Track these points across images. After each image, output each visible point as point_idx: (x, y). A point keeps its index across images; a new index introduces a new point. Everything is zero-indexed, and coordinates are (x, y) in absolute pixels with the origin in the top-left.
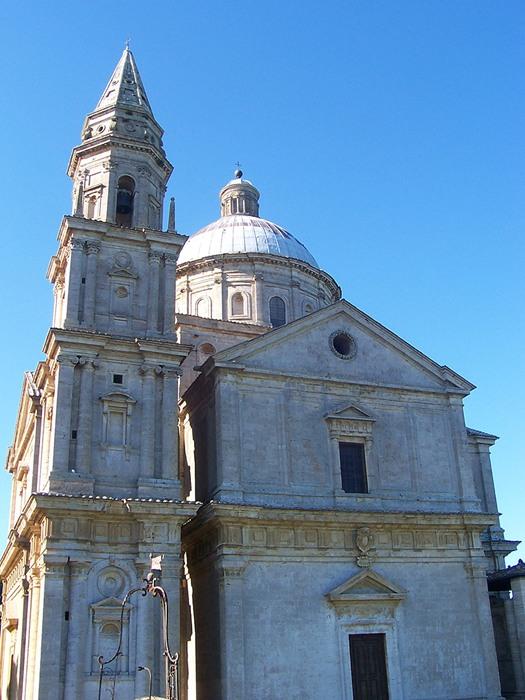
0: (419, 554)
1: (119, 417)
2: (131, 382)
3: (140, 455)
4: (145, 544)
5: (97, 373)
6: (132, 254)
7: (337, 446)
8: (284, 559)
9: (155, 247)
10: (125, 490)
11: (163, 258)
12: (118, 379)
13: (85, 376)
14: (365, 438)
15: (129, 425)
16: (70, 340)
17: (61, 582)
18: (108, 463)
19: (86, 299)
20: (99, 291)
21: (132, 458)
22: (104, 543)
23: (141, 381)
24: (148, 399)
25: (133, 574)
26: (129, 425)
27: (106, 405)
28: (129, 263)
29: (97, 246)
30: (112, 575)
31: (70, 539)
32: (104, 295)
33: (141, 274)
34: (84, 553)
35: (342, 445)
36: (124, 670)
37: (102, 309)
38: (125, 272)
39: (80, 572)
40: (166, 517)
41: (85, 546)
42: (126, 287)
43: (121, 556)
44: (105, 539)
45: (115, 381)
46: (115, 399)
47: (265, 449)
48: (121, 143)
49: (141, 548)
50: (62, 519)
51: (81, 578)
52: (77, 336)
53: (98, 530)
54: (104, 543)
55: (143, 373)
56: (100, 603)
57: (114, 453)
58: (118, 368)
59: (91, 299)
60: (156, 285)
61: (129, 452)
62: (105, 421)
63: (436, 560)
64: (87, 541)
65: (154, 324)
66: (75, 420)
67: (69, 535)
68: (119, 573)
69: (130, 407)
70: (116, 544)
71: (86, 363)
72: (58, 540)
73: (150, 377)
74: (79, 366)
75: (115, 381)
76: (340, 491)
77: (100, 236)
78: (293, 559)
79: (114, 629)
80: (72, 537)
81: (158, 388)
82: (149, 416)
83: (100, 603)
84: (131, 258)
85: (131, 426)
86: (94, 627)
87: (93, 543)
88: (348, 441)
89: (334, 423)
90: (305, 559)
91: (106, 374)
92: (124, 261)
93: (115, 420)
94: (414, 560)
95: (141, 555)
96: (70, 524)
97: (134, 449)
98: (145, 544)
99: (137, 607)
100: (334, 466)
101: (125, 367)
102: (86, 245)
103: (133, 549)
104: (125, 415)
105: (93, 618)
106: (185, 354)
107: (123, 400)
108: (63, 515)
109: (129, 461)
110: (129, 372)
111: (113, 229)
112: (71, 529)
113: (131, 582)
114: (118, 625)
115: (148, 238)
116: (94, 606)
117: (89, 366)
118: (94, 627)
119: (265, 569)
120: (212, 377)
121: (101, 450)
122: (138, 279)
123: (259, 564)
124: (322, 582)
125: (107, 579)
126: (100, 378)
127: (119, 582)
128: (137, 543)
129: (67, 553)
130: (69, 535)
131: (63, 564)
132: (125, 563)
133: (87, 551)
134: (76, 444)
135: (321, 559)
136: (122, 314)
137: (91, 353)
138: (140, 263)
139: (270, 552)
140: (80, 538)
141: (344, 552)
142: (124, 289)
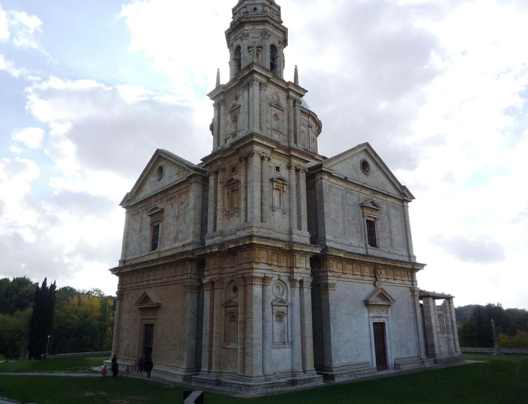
4: (296, 268)
6: (280, 95)
8: (349, 280)
9: (291, 94)
10: (285, 235)
11: (295, 101)
17: (261, 289)
23: (288, 172)
24: (294, 183)
25: (288, 285)
30: (279, 285)
36: (286, 341)
41: (271, 268)
42: (278, 115)
43: (283, 274)
48: (272, 22)
55: (289, 167)
65: (292, 139)
67: (264, 261)
70: (280, 267)
73: (293, 171)
78: (352, 280)
82: (294, 192)
84: (279, 97)
90: (356, 281)
92: (275, 98)
94: (392, 284)
95: (295, 274)
97: (287, 212)
98: (296, 268)
99: (292, 304)
103: (288, 270)
109: (284, 218)
114: (282, 314)
115: (290, 87)
116: (274, 303)
119: (341, 284)
122: (282, 110)
123: (340, 282)
124: (364, 295)
127: (281, 288)
128: (293, 267)
129: (263, 271)
133: (271, 270)
135: (362, 281)
138: (283, 102)
139: (344, 276)
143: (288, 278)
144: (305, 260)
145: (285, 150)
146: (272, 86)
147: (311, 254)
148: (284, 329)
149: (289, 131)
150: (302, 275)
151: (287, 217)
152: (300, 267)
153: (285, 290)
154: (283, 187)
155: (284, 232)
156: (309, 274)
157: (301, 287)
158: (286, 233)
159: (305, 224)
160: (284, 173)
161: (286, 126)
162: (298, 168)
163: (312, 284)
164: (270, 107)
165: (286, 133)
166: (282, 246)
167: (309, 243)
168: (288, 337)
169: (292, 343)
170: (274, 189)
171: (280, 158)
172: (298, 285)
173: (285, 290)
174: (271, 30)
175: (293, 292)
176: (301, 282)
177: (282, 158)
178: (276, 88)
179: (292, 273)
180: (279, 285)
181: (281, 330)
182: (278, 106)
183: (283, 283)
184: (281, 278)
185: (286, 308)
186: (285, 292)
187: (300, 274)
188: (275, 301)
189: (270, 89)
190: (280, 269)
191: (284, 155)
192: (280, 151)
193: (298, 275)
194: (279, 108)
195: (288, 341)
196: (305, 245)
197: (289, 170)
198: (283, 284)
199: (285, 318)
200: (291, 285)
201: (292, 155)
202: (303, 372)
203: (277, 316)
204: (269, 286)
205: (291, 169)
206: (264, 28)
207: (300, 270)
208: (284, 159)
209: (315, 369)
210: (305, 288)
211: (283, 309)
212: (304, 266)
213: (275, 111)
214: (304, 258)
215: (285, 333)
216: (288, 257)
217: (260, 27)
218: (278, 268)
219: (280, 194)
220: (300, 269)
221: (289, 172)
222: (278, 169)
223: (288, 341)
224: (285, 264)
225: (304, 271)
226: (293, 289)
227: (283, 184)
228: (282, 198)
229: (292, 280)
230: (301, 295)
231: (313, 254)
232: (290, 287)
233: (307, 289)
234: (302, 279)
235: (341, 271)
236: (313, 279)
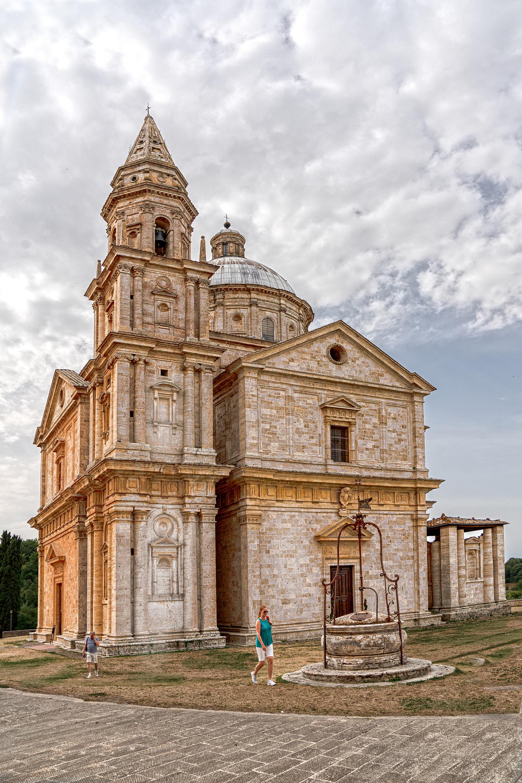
0: (381, 508)
1: (166, 403)
2: (174, 377)
3: (183, 431)
4: (190, 497)
5: (148, 368)
6: (171, 279)
7: (329, 429)
12: (164, 373)
13: (138, 370)
14: (349, 422)
15: (174, 408)
16: (126, 342)
18: (159, 436)
19: (136, 312)
20: (145, 306)
21: (177, 432)
22: (158, 496)
23: (182, 375)
25: (180, 520)
26: (174, 408)
27: (156, 392)
28: (169, 285)
29: (143, 271)
30: (165, 520)
31: (134, 494)
32: (150, 309)
33: (180, 294)
34: (145, 504)
35: (333, 428)
37: (149, 319)
38: (166, 292)
39: (142, 518)
40: (206, 477)
42: (168, 304)
44: (159, 493)
45: (162, 375)
46: (162, 388)
47: (276, 428)
49: (187, 500)
50: (127, 478)
51: (143, 524)
52: (132, 339)
53: (154, 486)
54: (158, 496)
55: (184, 369)
56: (157, 542)
57: (163, 431)
58: (163, 364)
59: (140, 312)
60: (192, 301)
61: (175, 428)
62: (155, 404)
63: (392, 512)
64: (147, 494)
66: (133, 403)
68: (168, 519)
69: (175, 394)
70: (167, 497)
71: (140, 360)
72: (124, 494)
74: (133, 363)
75: (162, 375)
76: (330, 462)
77: (144, 263)
79: (165, 561)
80: (136, 492)
81: (196, 381)
82: (191, 401)
83: (157, 542)
85: (176, 408)
86: (152, 560)
87: (151, 496)
88: (337, 424)
89: (328, 411)
91: (154, 369)
93: (164, 404)
96: (133, 481)
98: (190, 497)
99: (184, 545)
100: (326, 441)
101: (170, 364)
102: (132, 270)
103: (180, 501)
104: (170, 400)
105: (152, 552)
106: (218, 356)
107: (169, 389)
108: (127, 475)
109: (175, 434)
110: (174, 368)
111: (155, 258)
112: (134, 485)
113: (178, 526)
116: (154, 544)
117: (141, 362)
118: (152, 560)
120: (236, 376)
121: (156, 426)
125: (160, 524)
126: (150, 372)
127: (170, 526)
128: (185, 496)
130: (133, 490)
131: (127, 512)
132: (174, 511)
134: (134, 421)
136: (166, 324)
137: (143, 353)
140: (142, 492)
141: (331, 506)
142: (165, 305)
143: (179, 512)
144: (205, 485)
145: (172, 347)
146: (157, 270)
147: (215, 477)
148: (173, 577)
149: (187, 321)
150: (200, 506)
151: (179, 433)
152: (195, 496)
153: (175, 526)
154: (172, 395)
155: (171, 452)
156: (213, 504)
157: (199, 523)
158: (175, 452)
159: (208, 439)
160: (174, 377)
161: (182, 316)
162: (198, 367)
163: (218, 518)
164: (153, 297)
165: (182, 325)
166: (160, 470)
167: (215, 464)
168: (178, 587)
169: (183, 595)
170: (155, 399)
171: (169, 358)
172: (192, 519)
173: (175, 526)
174: (157, 200)
175: (185, 529)
176: (199, 515)
177: (172, 359)
178: (163, 271)
179: (184, 504)
180: (165, 520)
181: (168, 578)
182: (166, 292)
183: (171, 519)
184: (168, 512)
185: (175, 550)
186: (175, 530)
187: (196, 505)
188: (155, 540)
189: (153, 274)
190: (165, 500)
191: (174, 353)
192: (165, 350)
193: (192, 506)
194: (168, 295)
195: (178, 593)
196: (208, 466)
197: (185, 372)
198: (172, 520)
199: (174, 562)
200: (184, 519)
201: (185, 353)
202: (199, 632)
203: (161, 561)
204: (142, 523)
205: (187, 371)
206: (146, 198)
207: (196, 500)
208: (176, 359)
209: (218, 629)
210: (204, 522)
211: (167, 551)
212: (203, 494)
213: (160, 300)
214: (205, 483)
215: (173, 581)
216: (180, 484)
217: (140, 199)
218: (161, 499)
219: (169, 405)
220: (196, 499)
221: (185, 375)
222: (164, 373)
223: (178, 593)
224: (174, 493)
225: (202, 501)
226: (185, 525)
227: (173, 391)
228: (171, 408)
229: (185, 515)
230: (199, 534)
231: (219, 478)
232: (183, 523)
233: (208, 524)
234: (199, 511)
235: (274, 498)
236: (219, 510)
